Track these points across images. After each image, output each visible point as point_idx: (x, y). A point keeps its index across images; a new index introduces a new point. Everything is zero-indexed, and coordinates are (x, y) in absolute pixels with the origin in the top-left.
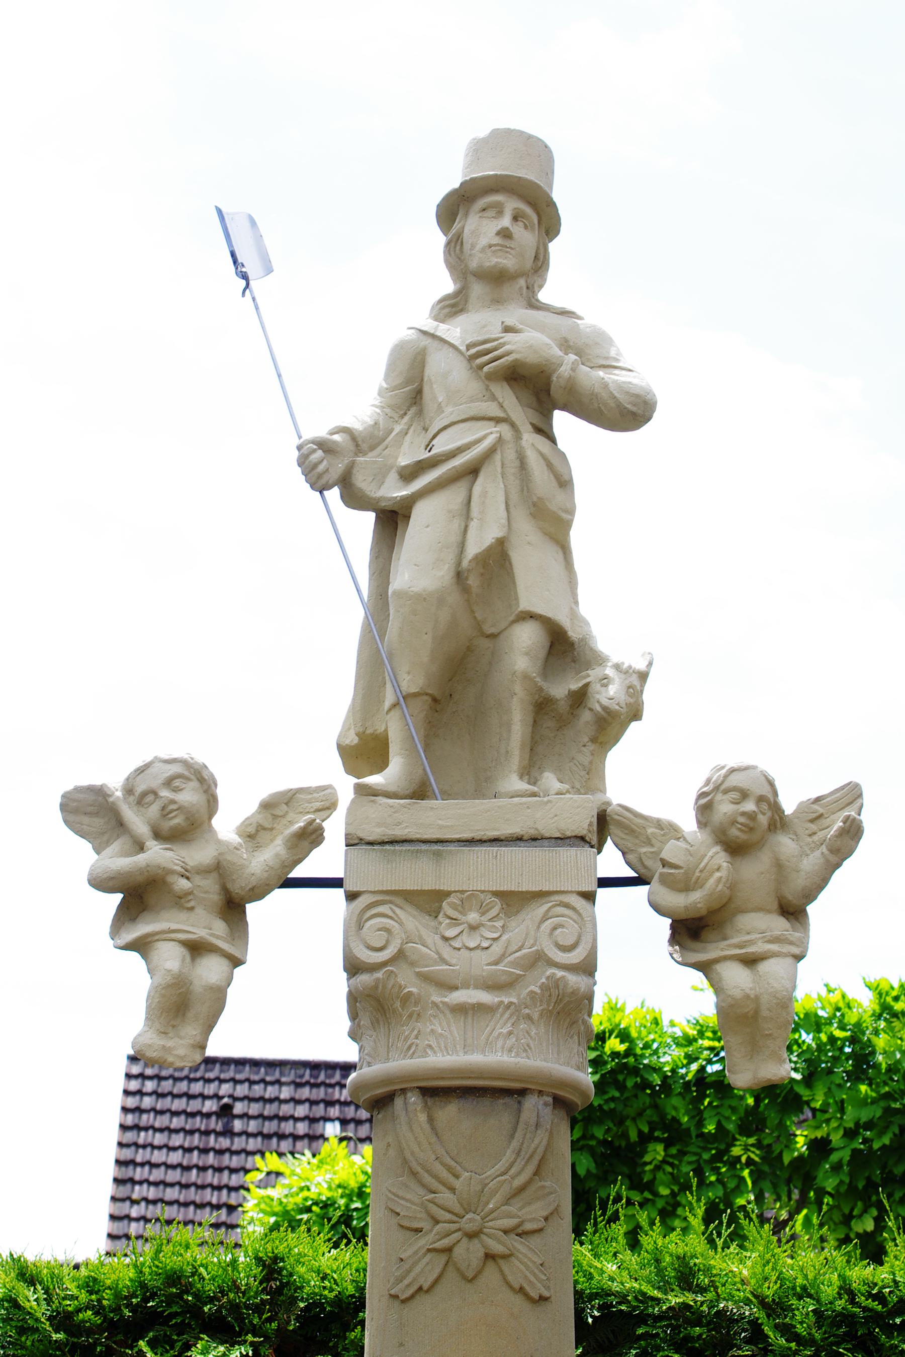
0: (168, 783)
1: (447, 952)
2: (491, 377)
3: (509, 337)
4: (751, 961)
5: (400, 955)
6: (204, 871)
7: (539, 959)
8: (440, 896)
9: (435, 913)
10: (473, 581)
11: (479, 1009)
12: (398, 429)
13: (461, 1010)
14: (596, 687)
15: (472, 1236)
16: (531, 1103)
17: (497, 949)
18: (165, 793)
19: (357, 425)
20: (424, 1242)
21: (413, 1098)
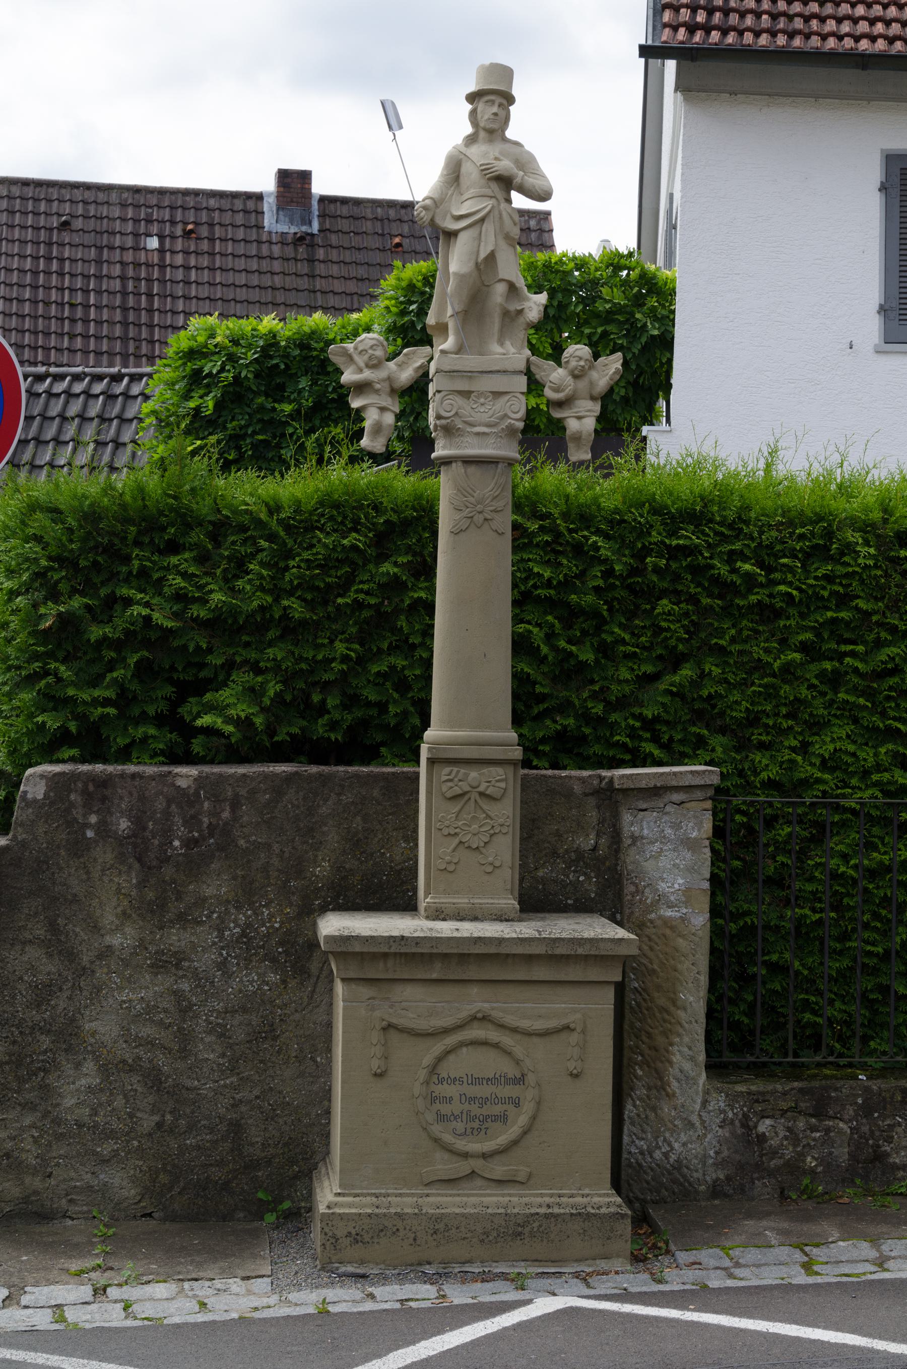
0: (371, 347)
1: (473, 414)
2: (489, 179)
3: (496, 163)
4: (579, 418)
5: (457, 413)
6: (384, 380)
7: (506, 416)
8: (471, 392)
9: (469, 398)
10: (482, 267)
11: (484, 434)
12: (450, 193)
13: (478, 434)
14: (526, 310)
15: (480, 512)
16: (500, 466)
17: (491, 412)
18: (370, 351)
19: (436, 196)
20: (465, 514)
21: (460, 464)
